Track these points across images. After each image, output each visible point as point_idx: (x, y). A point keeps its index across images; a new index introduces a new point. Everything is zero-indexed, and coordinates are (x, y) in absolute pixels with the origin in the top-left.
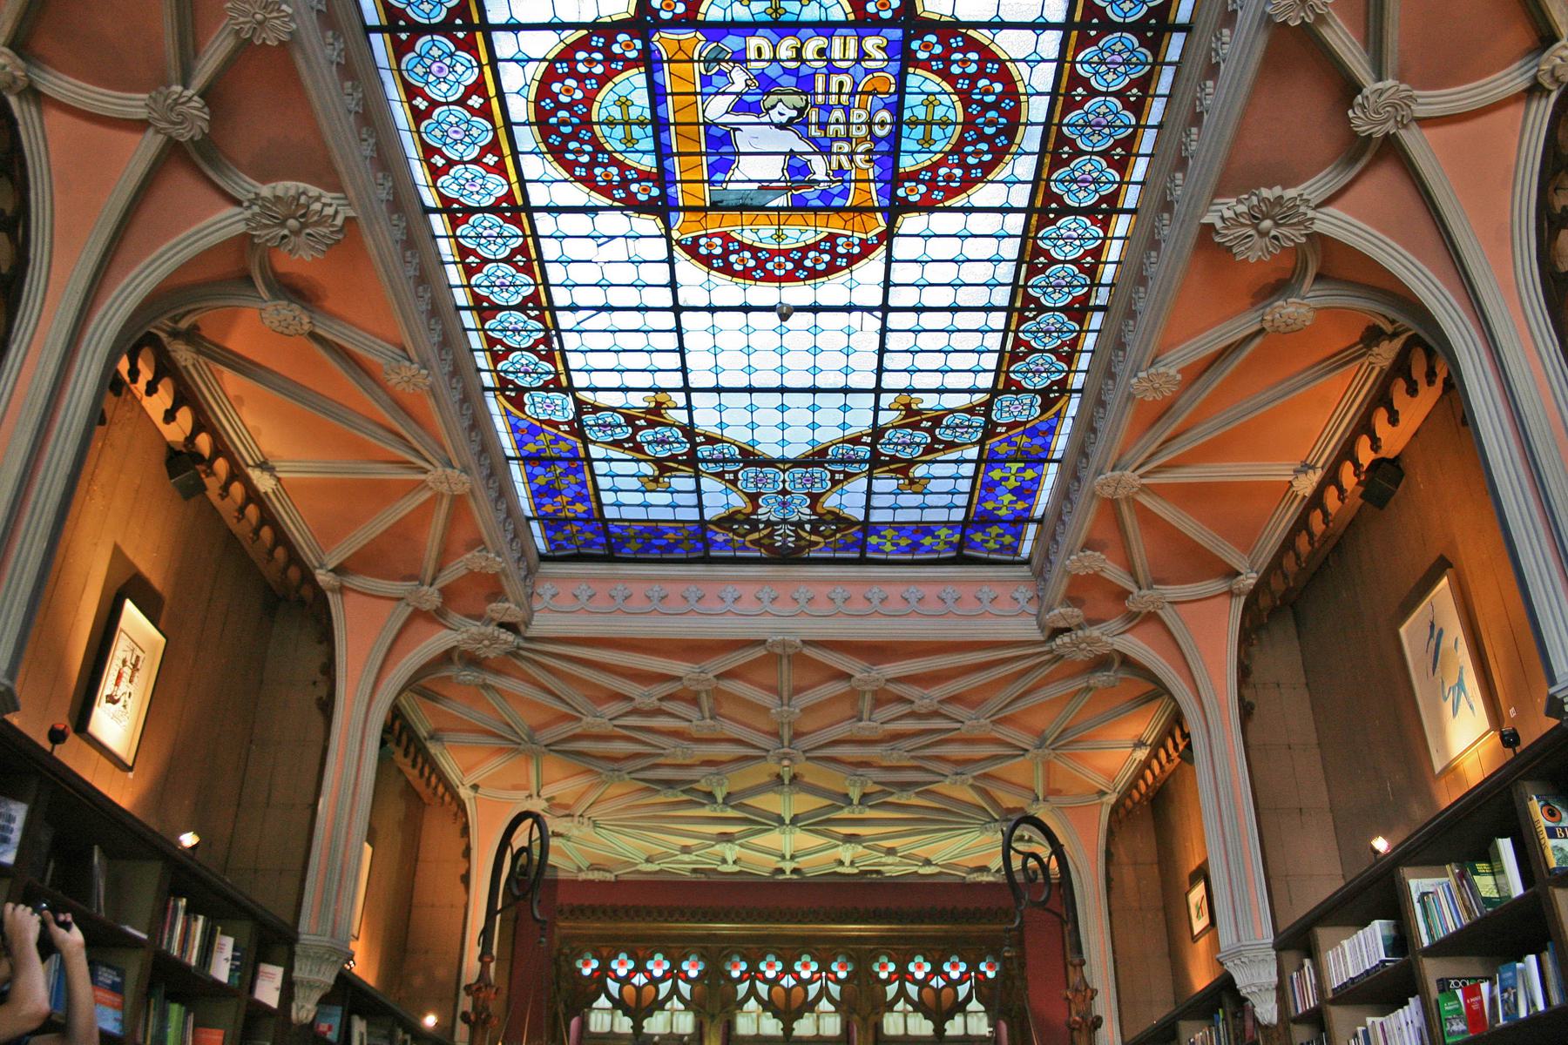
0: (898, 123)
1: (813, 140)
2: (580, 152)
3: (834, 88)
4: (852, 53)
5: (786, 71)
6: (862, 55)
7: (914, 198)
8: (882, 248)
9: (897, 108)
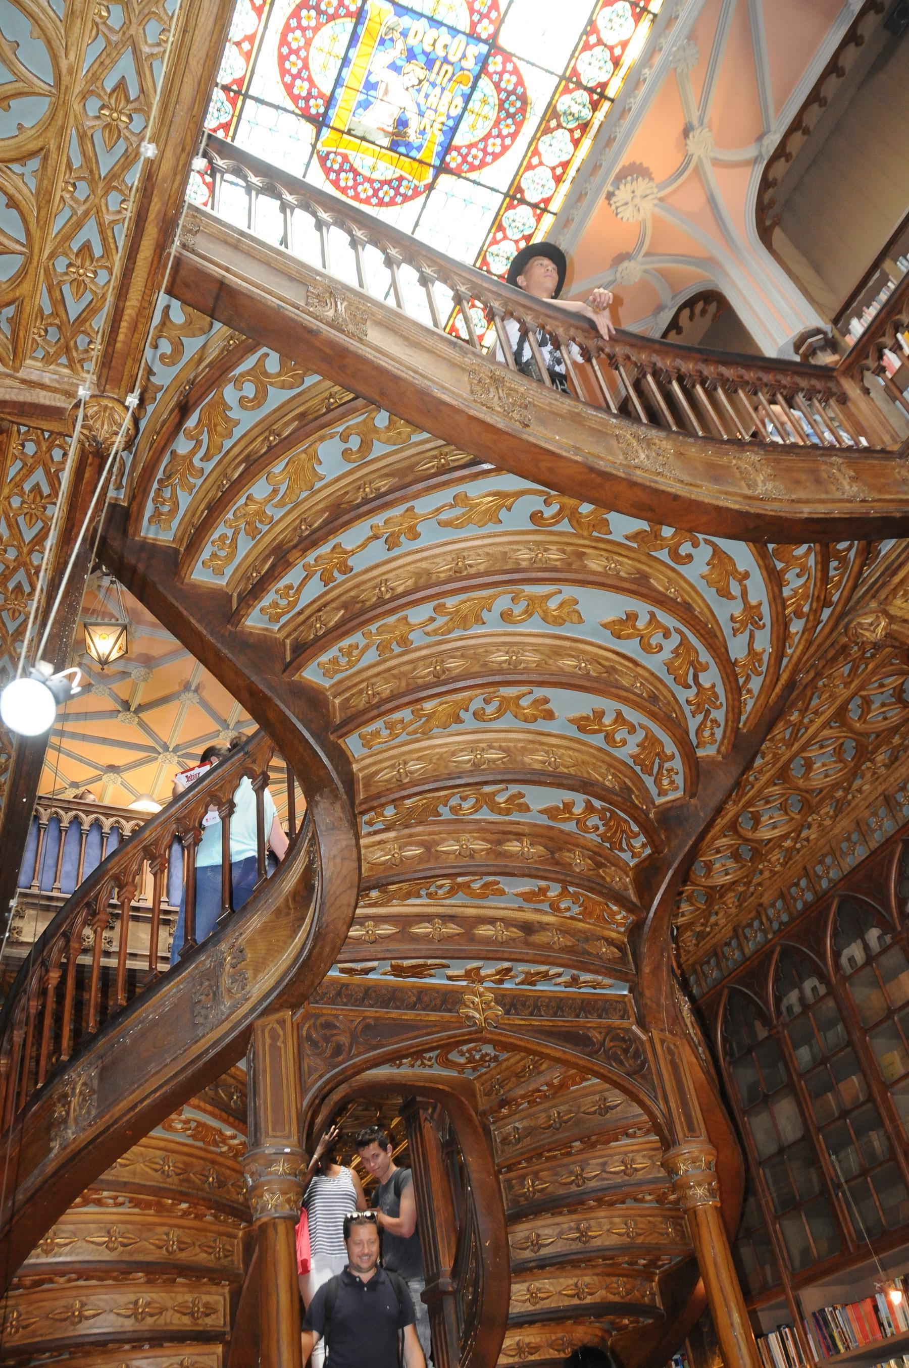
0: (465, 109)
1: (418, 105)
2: (294, 64)
3: (442, 73)
4: (459, 55)
5: (424, 52)
6: (464, 56)
7: (453, 165)
8: (424, 195)
9: (467, 98)
